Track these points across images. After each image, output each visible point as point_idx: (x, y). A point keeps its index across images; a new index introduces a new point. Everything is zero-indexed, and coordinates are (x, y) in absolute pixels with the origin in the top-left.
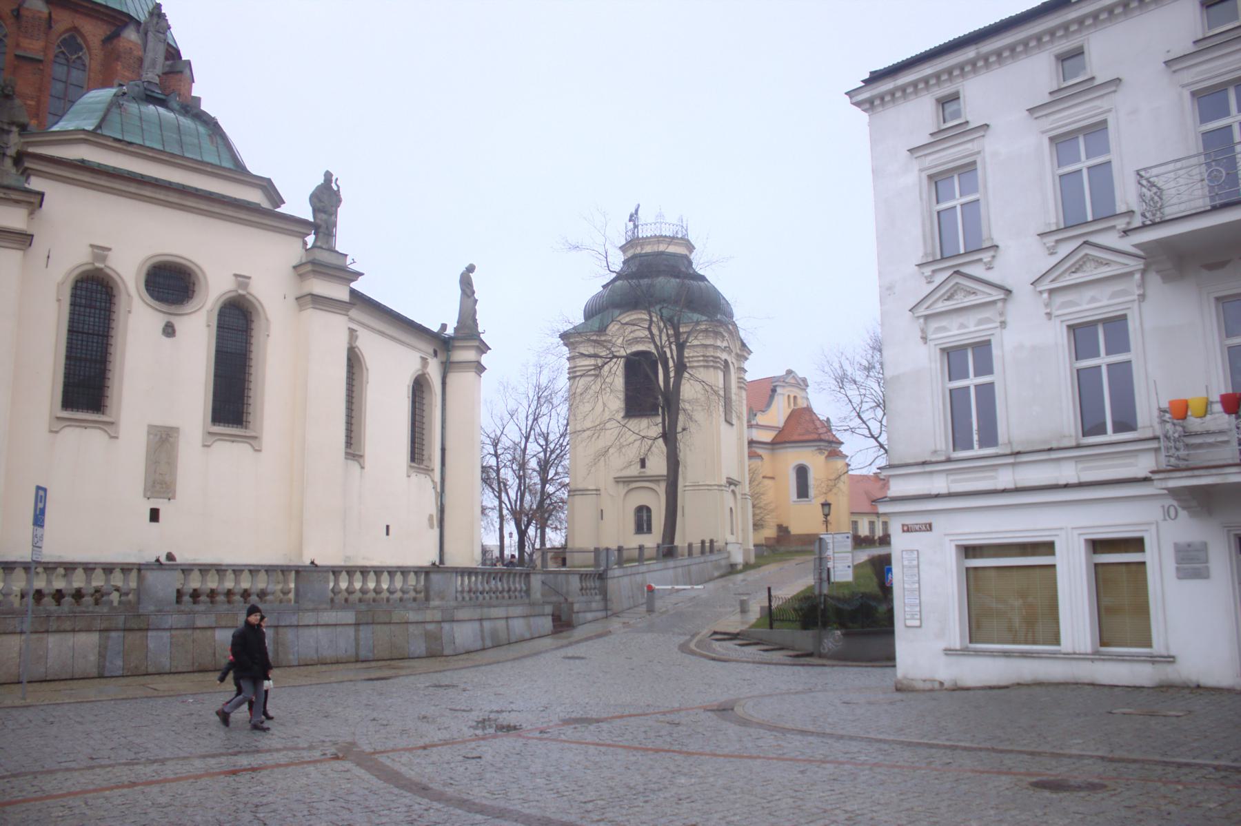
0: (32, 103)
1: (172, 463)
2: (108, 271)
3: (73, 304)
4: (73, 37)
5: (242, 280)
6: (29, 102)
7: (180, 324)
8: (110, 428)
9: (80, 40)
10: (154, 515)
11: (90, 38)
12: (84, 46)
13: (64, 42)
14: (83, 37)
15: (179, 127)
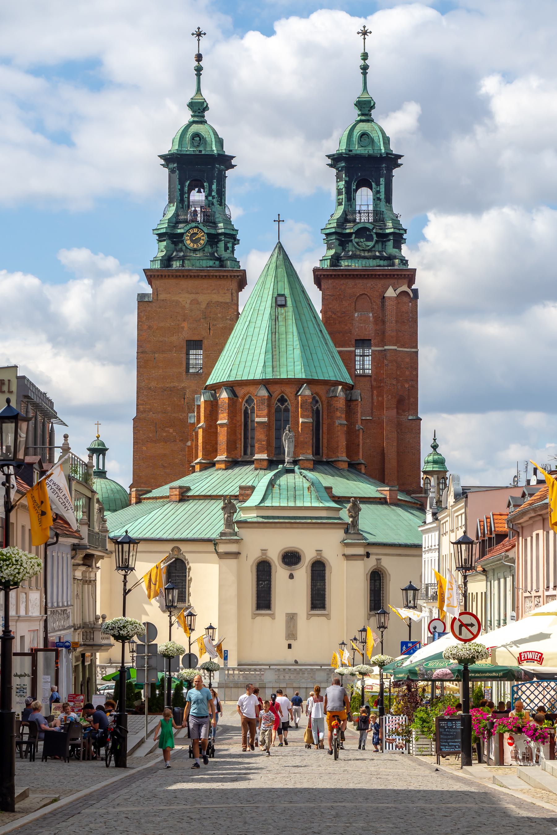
0: (264, 443)
1: (295, 626)
2: (268, 558)
3: (258, 571)
4: (282, 397)
5: (319, 551)
6: (263, 443)
7: (295, 574)
8: (272, 616)
9: (286, 397)
10: (290, 646)
11: (290, 395)
13: (279, 401)
15: (295, 488)
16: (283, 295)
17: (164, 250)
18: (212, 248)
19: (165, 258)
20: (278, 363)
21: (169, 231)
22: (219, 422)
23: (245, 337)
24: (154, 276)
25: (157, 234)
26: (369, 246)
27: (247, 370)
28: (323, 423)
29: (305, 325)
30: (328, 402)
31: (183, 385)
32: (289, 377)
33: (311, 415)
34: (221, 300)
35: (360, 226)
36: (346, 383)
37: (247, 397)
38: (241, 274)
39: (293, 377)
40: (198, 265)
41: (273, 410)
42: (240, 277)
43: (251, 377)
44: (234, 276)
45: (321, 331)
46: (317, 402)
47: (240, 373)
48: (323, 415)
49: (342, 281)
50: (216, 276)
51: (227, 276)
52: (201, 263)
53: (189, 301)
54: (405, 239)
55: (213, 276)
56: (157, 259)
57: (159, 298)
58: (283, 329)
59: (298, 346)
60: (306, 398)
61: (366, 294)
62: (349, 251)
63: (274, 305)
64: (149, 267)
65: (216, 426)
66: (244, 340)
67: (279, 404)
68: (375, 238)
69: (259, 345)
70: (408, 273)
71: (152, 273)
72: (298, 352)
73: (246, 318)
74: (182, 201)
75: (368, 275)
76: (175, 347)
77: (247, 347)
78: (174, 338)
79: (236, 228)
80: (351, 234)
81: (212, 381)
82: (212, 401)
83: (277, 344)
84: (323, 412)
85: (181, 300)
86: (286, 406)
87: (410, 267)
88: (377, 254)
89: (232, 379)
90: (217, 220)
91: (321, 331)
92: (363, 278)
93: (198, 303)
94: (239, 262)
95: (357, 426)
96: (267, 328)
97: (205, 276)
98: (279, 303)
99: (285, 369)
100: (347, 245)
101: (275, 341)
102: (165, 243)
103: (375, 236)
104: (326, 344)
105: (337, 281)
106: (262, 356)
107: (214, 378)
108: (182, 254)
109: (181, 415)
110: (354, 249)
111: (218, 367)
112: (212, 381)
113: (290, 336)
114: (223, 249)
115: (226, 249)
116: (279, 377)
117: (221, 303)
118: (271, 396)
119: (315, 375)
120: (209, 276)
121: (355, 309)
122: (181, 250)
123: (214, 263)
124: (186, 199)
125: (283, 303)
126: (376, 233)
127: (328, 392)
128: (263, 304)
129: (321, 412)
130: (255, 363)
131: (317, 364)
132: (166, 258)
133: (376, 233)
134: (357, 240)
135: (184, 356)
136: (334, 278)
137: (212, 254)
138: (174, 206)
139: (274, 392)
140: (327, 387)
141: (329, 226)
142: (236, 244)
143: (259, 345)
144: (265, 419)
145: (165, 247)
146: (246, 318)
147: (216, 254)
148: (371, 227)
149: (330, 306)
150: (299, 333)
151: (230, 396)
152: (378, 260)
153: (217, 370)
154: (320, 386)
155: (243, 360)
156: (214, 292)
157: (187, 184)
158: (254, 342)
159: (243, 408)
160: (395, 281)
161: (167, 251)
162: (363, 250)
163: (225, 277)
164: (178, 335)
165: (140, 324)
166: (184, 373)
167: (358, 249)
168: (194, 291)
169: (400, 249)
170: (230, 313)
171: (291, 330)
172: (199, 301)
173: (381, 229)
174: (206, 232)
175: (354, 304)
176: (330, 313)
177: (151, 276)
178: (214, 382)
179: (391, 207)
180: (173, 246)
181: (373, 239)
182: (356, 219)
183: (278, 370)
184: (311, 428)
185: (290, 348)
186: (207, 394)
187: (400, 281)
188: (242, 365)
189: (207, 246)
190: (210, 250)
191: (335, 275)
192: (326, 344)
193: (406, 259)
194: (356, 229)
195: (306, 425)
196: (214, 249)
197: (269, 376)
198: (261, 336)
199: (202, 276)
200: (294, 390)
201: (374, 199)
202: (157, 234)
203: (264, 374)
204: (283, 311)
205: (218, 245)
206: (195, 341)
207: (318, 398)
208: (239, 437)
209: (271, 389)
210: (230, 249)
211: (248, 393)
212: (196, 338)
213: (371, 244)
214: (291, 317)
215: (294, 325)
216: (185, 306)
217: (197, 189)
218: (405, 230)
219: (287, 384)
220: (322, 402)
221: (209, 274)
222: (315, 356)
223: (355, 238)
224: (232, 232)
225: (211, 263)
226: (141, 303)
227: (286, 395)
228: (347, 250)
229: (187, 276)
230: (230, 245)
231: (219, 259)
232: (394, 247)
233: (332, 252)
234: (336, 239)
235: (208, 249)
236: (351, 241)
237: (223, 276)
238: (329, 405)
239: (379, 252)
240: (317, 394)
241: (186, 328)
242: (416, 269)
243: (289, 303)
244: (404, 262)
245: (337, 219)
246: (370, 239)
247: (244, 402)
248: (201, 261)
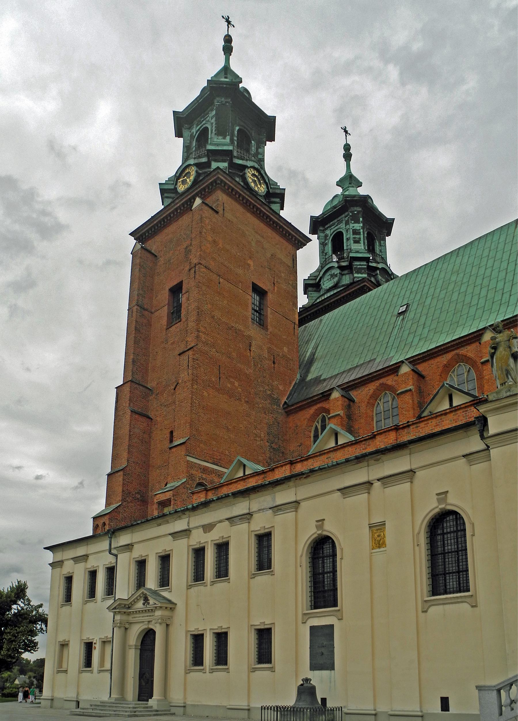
51: (293, 236)
71: (224, 179)
78: (240, 271)
85: (247, 232)
97: (274, 222)
156: (277, 246)
157: (237, 128)
177: (222, 181)
199: (271, 219)
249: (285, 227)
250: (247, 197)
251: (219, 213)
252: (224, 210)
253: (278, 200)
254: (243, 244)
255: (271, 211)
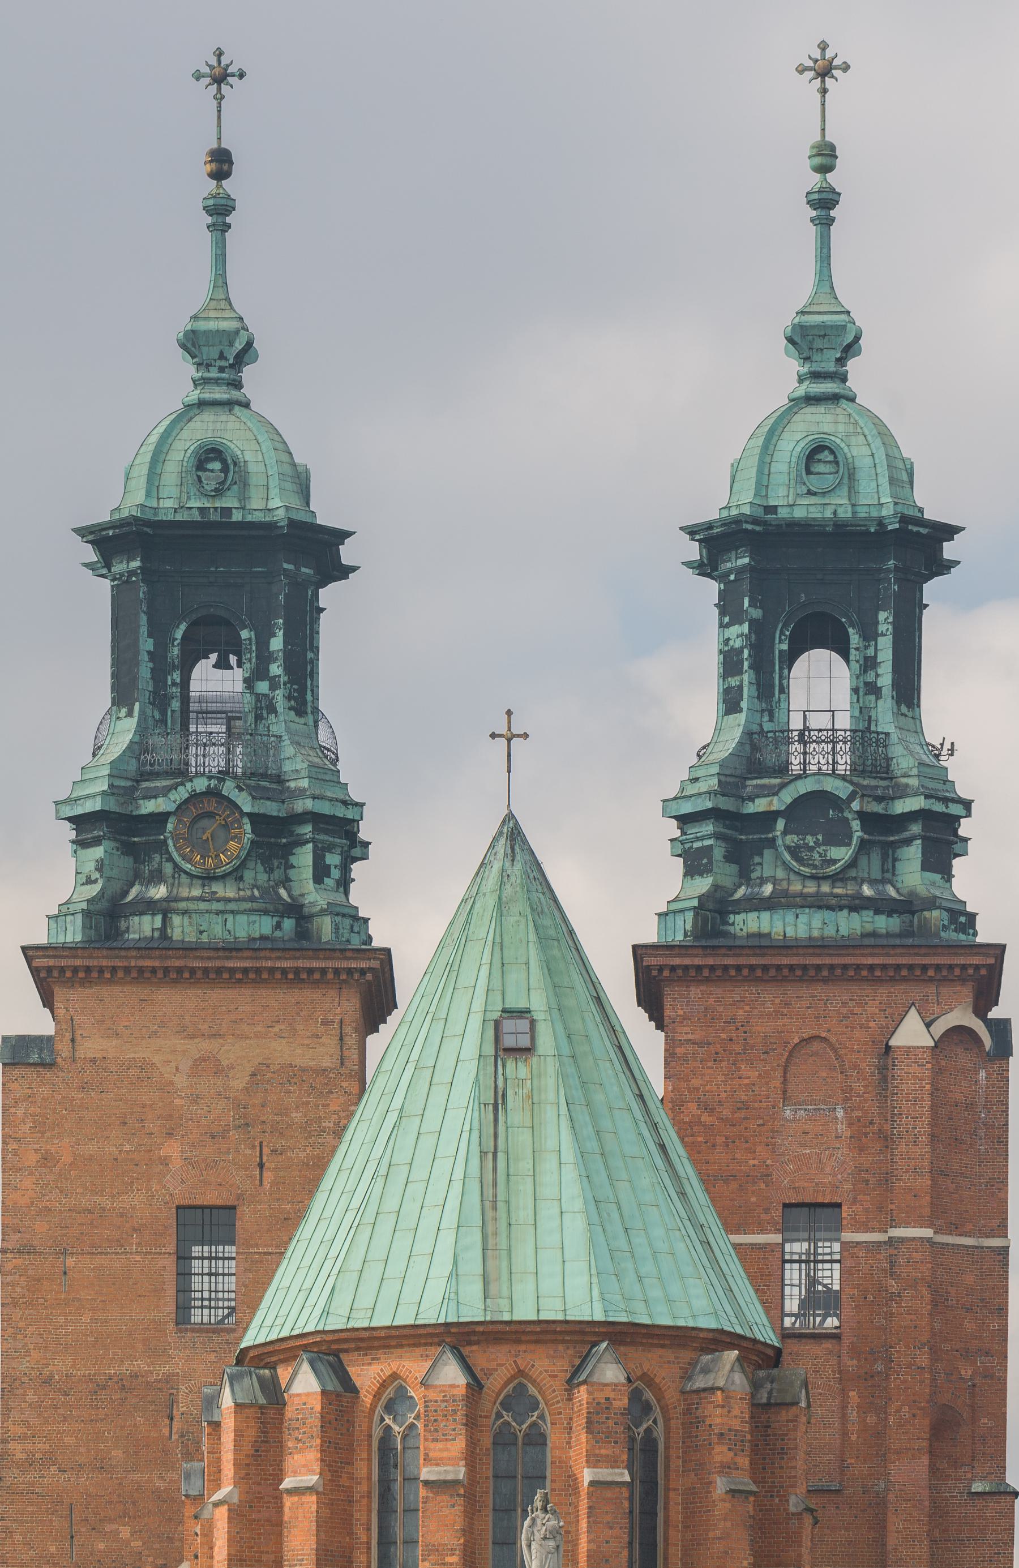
0: (454, 1559)
4: (521, 1389)
6: (449, 1559)
9: (532, 1390)
12: (540, 1398)
13: (506, 1405)
14: (534, 1382)
16: (523, 1013)
17: (96, 875)
18: (270, 870)
19: (98, 907)
20: (505, 1264)
21: (112, 806)
22: (287, 1483)
23: (383, 1171)
24: (62, 970)
25: (70, 819)
26: (834, 862)
27: (391, 1290)
28: (667, 1489)
29: (606, 1124)
30: (687, 1412)
31: (166, 1369)
32: (543, 1317)
33: (625, 1457)
34: (302, 1057)
35: (803, 787)
36: (755, 1341)
37: (389, 1392)
38: (375, 964)
39: (560, 1317)
40: (218, 930)
41: (486, 1440)
42: (369, 976)
43: (405, 1318)
44: (350, 971)
45: (662, 1147)
46: (647, 1408)
47: (365, 1301)
48: (667, 1458)
49: (738, 992)
50: (284, 971)
51: (323, 971)
52: (229, 925)
53: (185, 1065)
54: (966, 840)
55: (272, 970)
56: (73, 908)
57: (80, 1054)
58: (521, 1139)
59: (578, 1204)
60: (608, 1393)
61: (825, 1040)
62: (763, 881)
63: (490, 1049)
64: (42, 939)
65: (277, 1498)
66: (380, 1181)
67: (507, 1417)
68: (858, 834)
69: (435, 1197)
70: (976, 960)
71: (51, 962)
72: (576, 1226)
73: (387, 1099)
74: (159, 699)
75: (832, 967)
76: (135, 1230)
77: (391, 1203)
79: (355, 795)
80: (771, 816)
81: (264, 1331)
82: (261, 1407)
83: (501, 1196)
84: (667, 1448)
85: (156, 1060)
86: (534, 1424)
87: (985, 934)
88: (867, 891)
89: (335, 1323)
90: (287, 767)
91: (662, 1147)
92: (813, 980)
93: (220, 1071)
94: (366, 921)
95: (793, 1499)
96: (465, 1135)
97: (245, 971)
98: (509, 1041)
99: (531, 1286)
100: (757, 859)
101: (495, 1184)
102: (98, 852)
103: (856, 825)
104: (682, 1194)
105: (717, 991)
106: (447, 1239)
107: (268, 1322)
108: (160, 892)
109: (161, 1478)
110: (780, 874)
111: (286, 1283)
112: (264, 1331)
113: (549, 1164)
114: (308, 873)
115: (320, 873)
116: (506, 1317)
117: (303, 1070)
118: (481, 1387)
119: (640, 1307)
120: (258, 971)
121: (785, 1092)
122: (157, 877)
123: (278, 926)
124: (176, 691)
125: (524, 1042)
126: (861, 815)
127: (687, 1376)
128: (451, 1048)
129: (661, 1446)
130: (420, 1265)
131: (648, 1268)
132: (104, 904)
133: (861, 815)
134: (792, 839)
135: (170, 1263)
136: (707, 980)
137: (269, 893)
138: (130, 714)
139: (488, 1373)
140: (686, 1355)
141: (691, 790)
142: (355, 859)
143: (435, 1197)
144: (460, 1472)
145: (100, 867)
146: (387, 1099)
147: (282, 892)
148: (842, 789)
149: (695, 1082)
150: (583, 1154)
151: (330, 1388)
152: (868, 915)
153: (281, 1294)
154: (660, 1351)
155: (378, 1252)
156: (276, 1029)
158: (416, 1189)
159: (377, 1432)
160: (932, 989)
161: (109, 879)
162: (813, 877)
163: (317, 976)
164: (149, 1189)
165: (13, 1146)
166: (171, 1326)
167: (798, 874)
168: (204, 1027)
169: (947, 874)
170: (332, 1108)
171: (551, 1144)
172: (225, 1063)
173: (879, 799)
174: (247, 809)
175: (779, 1074)
176: (692, 1107)
177: (49, 970)
178: (273, 1337)
179: (917, 719)
180: (128, 862)
181: (851, 838)
182: (788, 763)
183: (505, 1292)
184: (626, 1504)
185: (548, 1211)
186: (247, 1381)
187: (945, 990)
188: (373, 1272)
189: (251, 864)
190: (262, 877)
191: (712, 968)
192: (682, 1194)
193: (970, 908)
194: (789, 800)
195: (608, 1494)
196: (277, 875)
197: (473, 1311)
198: (443, 1166)
199: (232, 971)
200: (562, 1366)
201: (855, 690)
202: (70, 819)
203: (453, 1305)
204: (523, 1071)
205: (293, 860)
206: (211, 1208)
207: (649, 1395)
208: (364, 1538)
209: (481, 1357)
210: (336, 873)
211: (395, 1376)
212: (212, 1198)
213: (842, 854)
214: (551, 1096)
215: (565, 1123)
216: (171, 1083)
217: (214, 657)
218: (967, 805)
219: (537, 1342)
220: (664, 1410)
221: (258, 964)
222: (639, 1240)
223: (785, 833)
224: (340, 812)
225: (265, 925)
226: (17, 1072)
227: (534, 1382)
228: (754, 875)
229: (180, 970)
230: (333, 859)
231: (296, 910)
232: (926, 866)
233: (703, 885)
234: (716, 836)
235: (256, 875)
236: (772, 843)
237: (310, 971)
238: (693, 1421)
239: (872, 882)
240: (647, 1379)
241: (176, 1163)
242: (1003, 947)
243: (546, 1041)
244: (963, 919)
245: (723, 763)
246: (839, 836)
247: (379, 1410)
248: (230, 918)
249: (284, 964)
250: (133, 964)
251: (59, 1060)
252: (73, 1040)
253: (307, 829)
254: (144, 1106)
255: (221, 953)
